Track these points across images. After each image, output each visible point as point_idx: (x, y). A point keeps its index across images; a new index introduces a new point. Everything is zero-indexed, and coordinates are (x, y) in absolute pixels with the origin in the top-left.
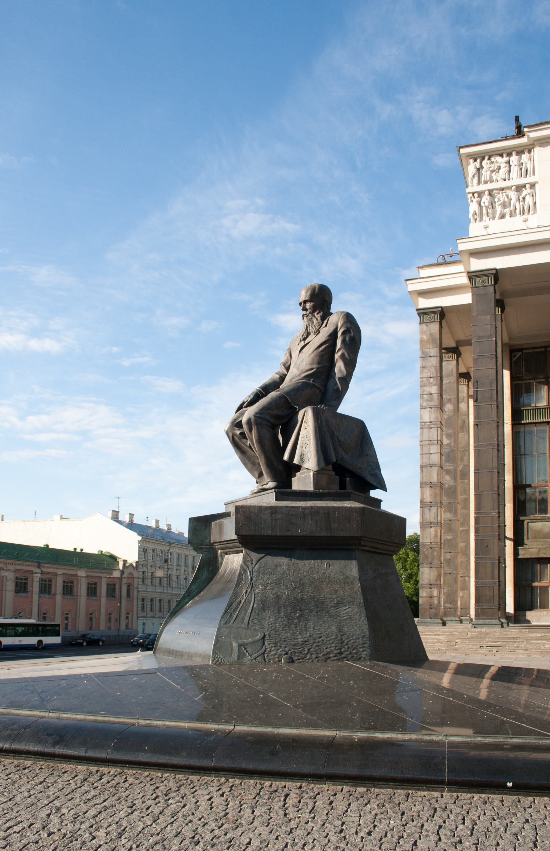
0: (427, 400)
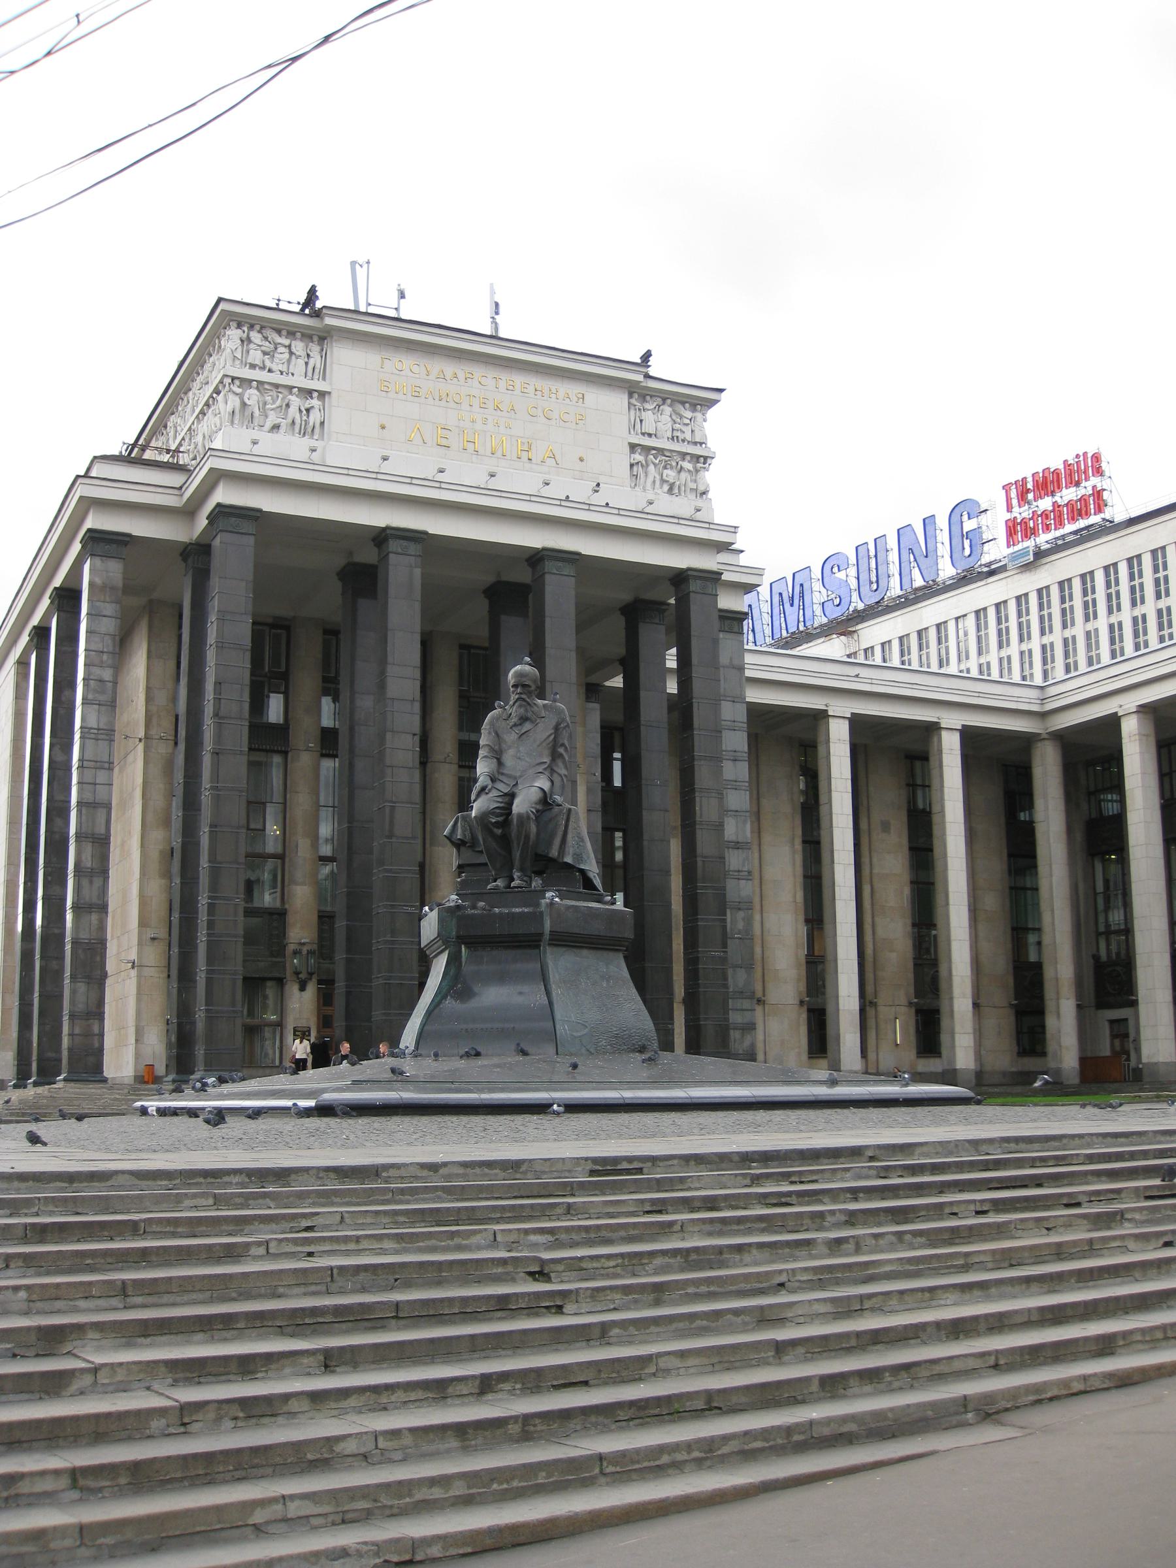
0: (96, 691)
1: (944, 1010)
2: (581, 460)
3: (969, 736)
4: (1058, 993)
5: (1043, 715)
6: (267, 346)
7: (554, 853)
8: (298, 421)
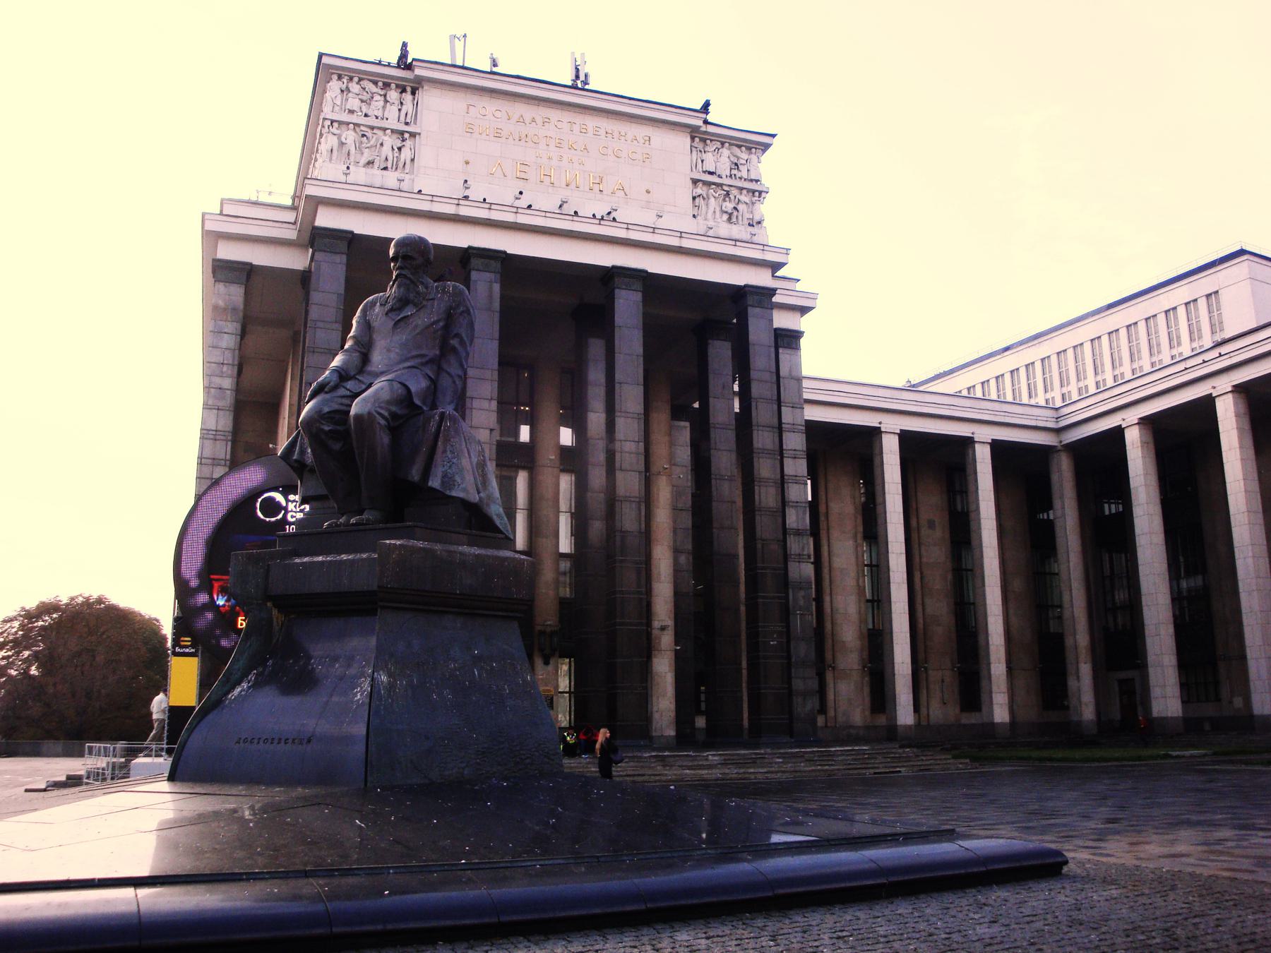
0: (216, 398)
1: (984, 673)
2: (648, 192)
3: (998, 448)
4: (1077, 658)
5: (1058, 431)
6: (366, 97)
7: (415, 474)
8: (390, 158)
